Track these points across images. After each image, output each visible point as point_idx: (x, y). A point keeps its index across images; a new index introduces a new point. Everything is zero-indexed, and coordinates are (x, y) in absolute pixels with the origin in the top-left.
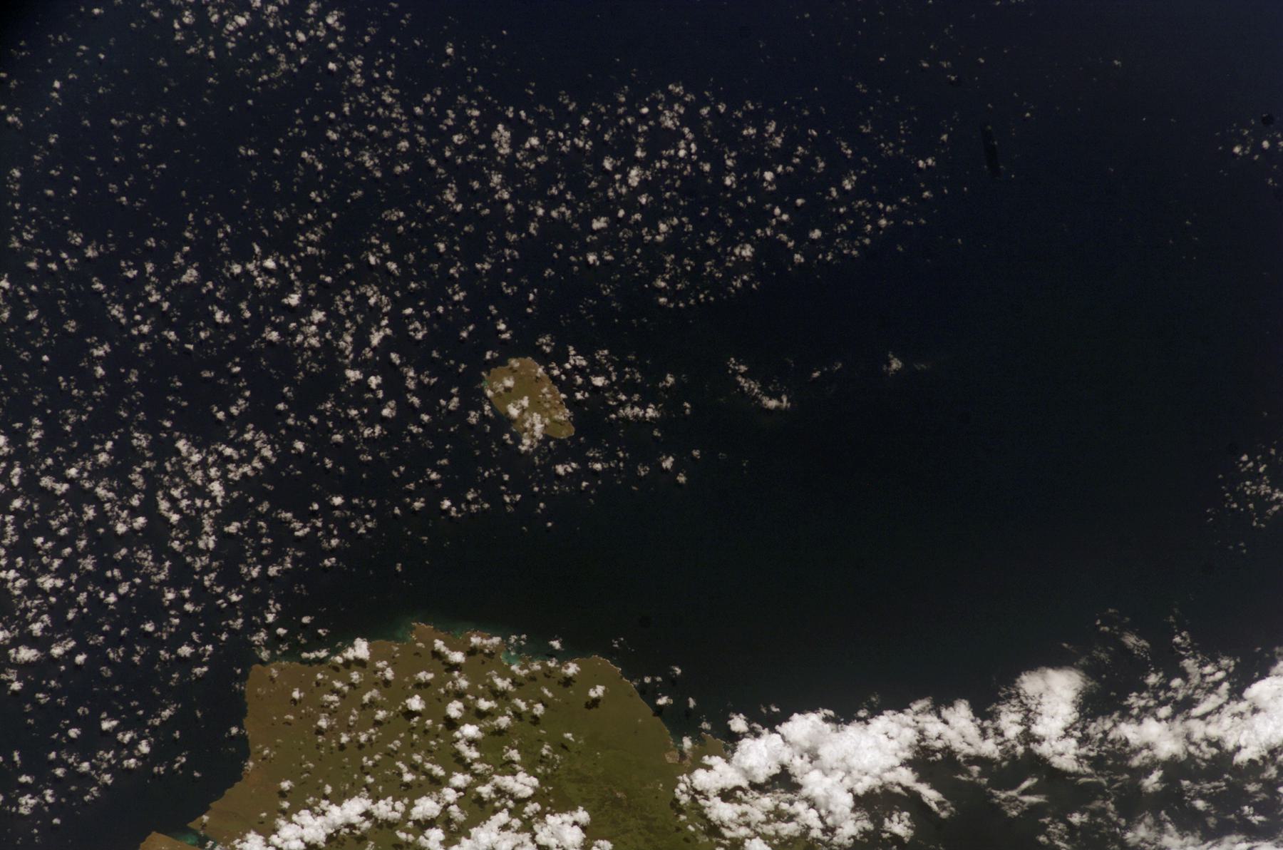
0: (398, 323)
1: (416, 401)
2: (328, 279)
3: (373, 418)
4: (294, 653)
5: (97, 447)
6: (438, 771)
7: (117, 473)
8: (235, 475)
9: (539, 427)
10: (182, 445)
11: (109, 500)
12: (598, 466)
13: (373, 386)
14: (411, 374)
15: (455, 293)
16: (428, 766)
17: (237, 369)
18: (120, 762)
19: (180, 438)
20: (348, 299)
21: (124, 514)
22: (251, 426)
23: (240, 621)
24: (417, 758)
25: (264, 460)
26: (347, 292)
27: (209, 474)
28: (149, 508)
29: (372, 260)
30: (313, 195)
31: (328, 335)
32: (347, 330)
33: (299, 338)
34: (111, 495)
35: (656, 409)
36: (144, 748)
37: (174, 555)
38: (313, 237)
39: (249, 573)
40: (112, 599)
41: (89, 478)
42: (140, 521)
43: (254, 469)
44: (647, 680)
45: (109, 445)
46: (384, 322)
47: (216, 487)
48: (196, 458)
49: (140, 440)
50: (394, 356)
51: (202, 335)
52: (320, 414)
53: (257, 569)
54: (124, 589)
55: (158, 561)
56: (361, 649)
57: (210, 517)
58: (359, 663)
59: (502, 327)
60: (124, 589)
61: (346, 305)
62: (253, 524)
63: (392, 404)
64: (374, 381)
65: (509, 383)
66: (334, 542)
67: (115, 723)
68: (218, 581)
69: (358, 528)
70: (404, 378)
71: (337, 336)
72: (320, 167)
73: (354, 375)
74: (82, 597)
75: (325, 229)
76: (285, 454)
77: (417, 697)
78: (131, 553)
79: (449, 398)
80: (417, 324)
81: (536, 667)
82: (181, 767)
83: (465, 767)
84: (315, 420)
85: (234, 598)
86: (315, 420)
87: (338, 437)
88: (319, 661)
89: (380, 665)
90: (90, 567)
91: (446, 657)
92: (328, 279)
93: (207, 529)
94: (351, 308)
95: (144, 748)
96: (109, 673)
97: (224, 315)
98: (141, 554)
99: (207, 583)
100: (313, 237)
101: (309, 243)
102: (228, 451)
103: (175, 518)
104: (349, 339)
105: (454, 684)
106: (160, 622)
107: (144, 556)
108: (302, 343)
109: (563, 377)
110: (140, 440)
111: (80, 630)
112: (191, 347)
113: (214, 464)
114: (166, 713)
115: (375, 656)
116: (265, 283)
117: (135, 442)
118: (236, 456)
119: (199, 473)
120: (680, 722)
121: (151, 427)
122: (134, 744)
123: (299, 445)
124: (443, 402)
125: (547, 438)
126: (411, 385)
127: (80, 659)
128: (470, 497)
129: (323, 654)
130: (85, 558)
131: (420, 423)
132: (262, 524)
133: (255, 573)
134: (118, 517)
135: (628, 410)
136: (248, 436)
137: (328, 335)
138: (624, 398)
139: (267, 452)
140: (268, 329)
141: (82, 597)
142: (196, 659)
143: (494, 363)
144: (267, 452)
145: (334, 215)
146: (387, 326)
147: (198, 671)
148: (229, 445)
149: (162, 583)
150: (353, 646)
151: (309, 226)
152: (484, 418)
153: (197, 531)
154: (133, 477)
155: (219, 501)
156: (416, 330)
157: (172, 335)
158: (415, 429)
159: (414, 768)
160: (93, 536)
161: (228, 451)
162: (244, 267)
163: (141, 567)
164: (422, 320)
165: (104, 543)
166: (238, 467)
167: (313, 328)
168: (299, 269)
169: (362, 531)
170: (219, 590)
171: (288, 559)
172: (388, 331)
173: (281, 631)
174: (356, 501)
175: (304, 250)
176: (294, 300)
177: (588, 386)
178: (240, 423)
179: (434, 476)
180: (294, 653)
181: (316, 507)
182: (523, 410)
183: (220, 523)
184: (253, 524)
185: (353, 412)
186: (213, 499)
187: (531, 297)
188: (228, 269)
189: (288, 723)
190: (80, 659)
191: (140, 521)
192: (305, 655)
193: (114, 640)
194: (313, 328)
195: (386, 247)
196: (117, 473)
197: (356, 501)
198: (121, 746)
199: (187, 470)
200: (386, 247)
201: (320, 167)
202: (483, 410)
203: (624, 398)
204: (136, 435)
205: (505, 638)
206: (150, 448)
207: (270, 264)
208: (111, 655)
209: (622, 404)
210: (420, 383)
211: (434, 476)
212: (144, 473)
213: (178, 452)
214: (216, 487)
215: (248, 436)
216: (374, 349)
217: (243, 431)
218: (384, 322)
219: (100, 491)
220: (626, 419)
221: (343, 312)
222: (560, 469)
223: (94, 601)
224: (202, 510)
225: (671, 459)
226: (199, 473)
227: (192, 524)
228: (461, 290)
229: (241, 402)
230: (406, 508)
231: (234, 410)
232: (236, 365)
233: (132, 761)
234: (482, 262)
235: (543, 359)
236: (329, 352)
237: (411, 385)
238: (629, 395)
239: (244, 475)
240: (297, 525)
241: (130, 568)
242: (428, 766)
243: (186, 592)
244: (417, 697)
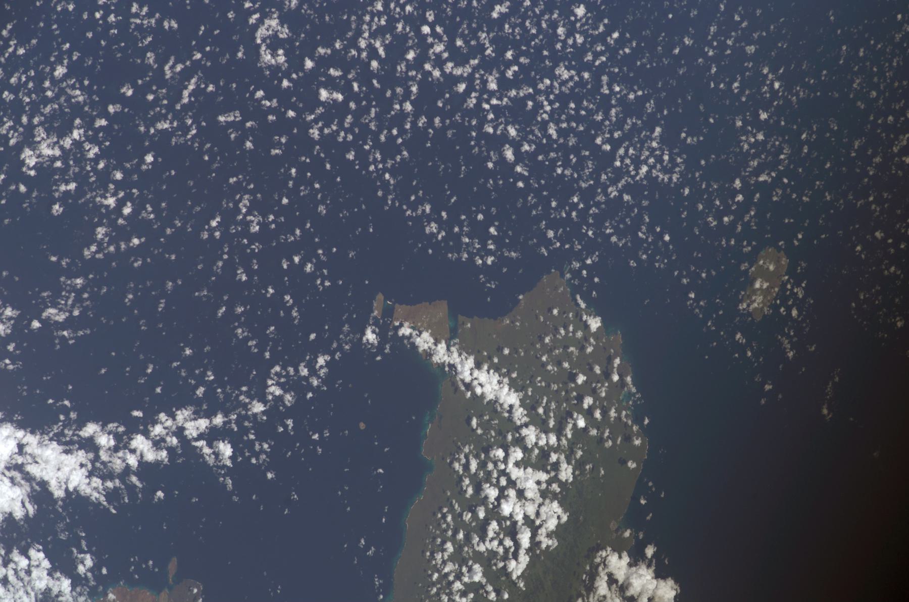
0: (777, 182)
1: (739, 228)
2: (783, 123)
3: (719, 217)
4: (575, 290)
5: (636, 88)
6: (552, 423)
7: (628, 109)
8: (655, 173)
9: (756, 305)
10: (658, 130)
11: (610, 121)
12: (749, 354)
13: (736, 200)
14: (753, 213)
15: (806, 196)
16: (552, 415)
17: (712, 121)
18: (476, 254)
19: (661, 126)
20: (777, 143)
21: (607, 136)
22: (685, 156)
23: (580, 247)
24: (553, 405)
25: (670, 179)
26: (780, 139)
27: (649, 161)
28: (616, 144)
29: (804, 136)
30: (825, 72)
31: (753, 151)
32: (760, 158)
33: (744, 138)
34: (614, 119)
35: (794, 355)
36: (490, 260)
37: (597, 180)
38: (802, 93)
39: (606, 228)
40: (559, 171)
41: (617, 100)
42: (607, 147)
43: (663, 179)
44: (650, 484)
45: (640, 93)
46: (773, 174)
47: (644, 169)
48: (654, 144)
49: (650, 106)
50: (758, 195)
51: (722, 86)
52: (709, 186)
53: (611, 231)
54: (568, 172)
55: (591, 176)
56: (595, 324)
57: (626, 181)
58: (586, 326)
59: (800, 236)
60: (568, 172)
61: (773, 145)
62: (633, 206)
63: (732, 218)
64: (740, 198)
65: (772, 268)
66: (644, 257)
67: (496, 233)
68: (595, 216)
69: (658, 261)
70: (748, 212)
71: (754, 157)
72: (841, 62)
73: (738, 183)
74: (553, 155)
75: (809, 95)
76: (680, 185)
77: (585, 378)
78: (588, 158)
79: (749, 244)
80: (780, 192)
81: (630, 422)
82: (490, 288)
83: (559, 432)
84: (704, 186)
85: (590, 233)
86: (704, 186)
87: (701, 207)
88: (578, 305)
89: (592, 340)
90: (571, 144)
91: (613, 372)
92: (783, 123)
93: (620, 185)
94: (773, 150)
95: (490, 260)
96: (519, 206)
97: (737, 88)
98: (590, 164)
99: (591, 212)
100: (802, 93)
101: (797, 94)
102: (666, 158)
103: (618, 164)
104: (756, 163)
105: (600, 388)
106: (560, 206)
107: (590, 166)
108: (741, 141)
109: (788, 293)
110: (650, 106)
111: (536, 169)
112: (712, 85)
113: (655, 157)
114: (513, 254)
115: (596, 335)
116: (765, 92)
117: (648, 104)
118: (665, 164)
119: (647, 153)
120: (634, 518)
121: (659, 108)
122: (490, 253)
123: (687, 191)
124: (745, 243)
125: (750, 314)
126: (747, 219)
127: (520, 184)
128: (701, 303)
129: (583, 305)
130: (574, 137)
131: (728, 241)
132: (636, 210)
133: (608, 231)
134: (604, 133)
135: (787, 341)
136: (679, 160)
137: (753, 151)
138: (792, 334)
139: (675, 177)
140: (740, 117)
141: (553, 155)
142: (549, 242)
143: (779, 249)
144: (675, 179)
145: (819, 94)
146: (772, 177)
147: (544, 250)
148: (670, 155)
149: (580, 188)
150: (595, 317)
151: (805, 86)
152: (747, 271)
153: (614, 182)
154: (629, 121)
155: (638, 178)
156: (777, 193)
157: (714, 70)
158: (723, 243)
159: (547, 410)
160: (587, 130)
161: (666, 158)
162: (768, 74)
163: (583, 170)
164: (784, 191)
165: (586, 140)
166: (660, 171)
167: (753, 140)
168: (781, 103)
169: (657, 265)
170: (591, 221)
171: (624, 241)
172: (770, 180)
173: (584, 272)
174: (671, 247)
175: (792, 96)
176: (764, 116)
177: (789, 310)
178: (686, 149)
179: (704, 275)
180: (575, 290)
181: (658, 230)
182: (761, 289)
183: (627, 189)
184: (633, 206)
185: (718, 203)
186: (637, 174)
187: (823, 236)
188: (764, 66)
189: (537, 317)
190: (520, 184)
191: (607, 147)
192: (578, 297)
193: (537, 193)
194: (753, 140)
195: (814, 137)
196: (628, 109)
197: (671, 247)
198: (484, 245)
199: (646, 145)
200: (814, 137)
201: (841, 62)
202: (751, 268)
203: (792, 334)
204: (652, 102)
205: (637, 392)
206: (649, 114)
207: (777, 85)
208: (530, 198)
209: (788, 336)
210: (749, 222)
211: (704, 275)
212: (634, 124)
213: (653, 131)
214: (644, 169)
215: (679, 160)
216: (757, 181)
217: (679, 155)
218: (773, 174)
219: (613, 111)
220: (781, 344)
221: (769, 146)
222: (738, 336)
223: (553, 162)
224: (628, 172)
225: (771, 387)
226: (647, 153)
227: (619, 174)
228: (810, 197)
229: (695, 139)
230: (680, 276)
231: (689, 140)
232: (714, 118)
233: (480, 262)
234: (830, 194)
235: (791, 272)
236: (745, 158)
237: (747, 219)
238: (795, 335)
239: (658, 176)
240: (644, 228)
241: (580, 166)
242: (552, 415)
243: (582, 206)
244: (585, 378)
